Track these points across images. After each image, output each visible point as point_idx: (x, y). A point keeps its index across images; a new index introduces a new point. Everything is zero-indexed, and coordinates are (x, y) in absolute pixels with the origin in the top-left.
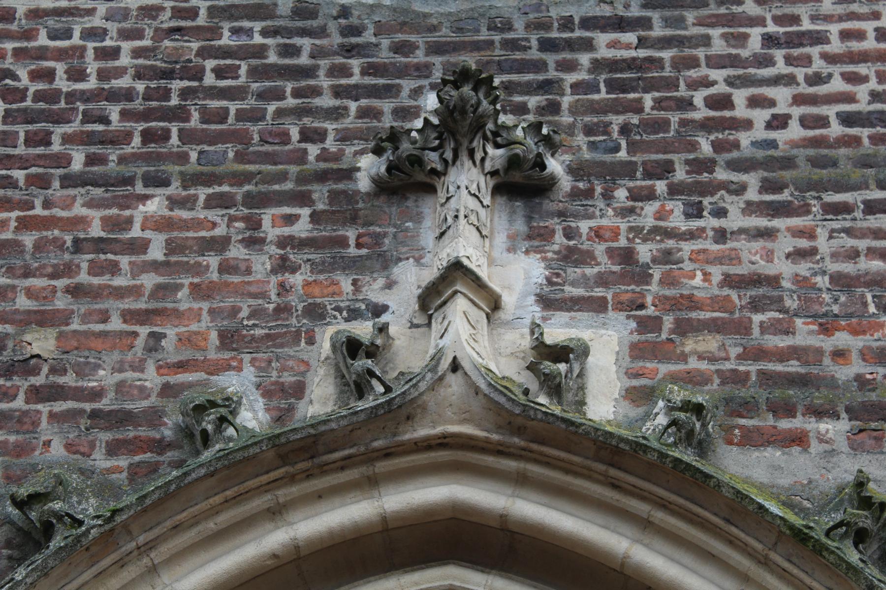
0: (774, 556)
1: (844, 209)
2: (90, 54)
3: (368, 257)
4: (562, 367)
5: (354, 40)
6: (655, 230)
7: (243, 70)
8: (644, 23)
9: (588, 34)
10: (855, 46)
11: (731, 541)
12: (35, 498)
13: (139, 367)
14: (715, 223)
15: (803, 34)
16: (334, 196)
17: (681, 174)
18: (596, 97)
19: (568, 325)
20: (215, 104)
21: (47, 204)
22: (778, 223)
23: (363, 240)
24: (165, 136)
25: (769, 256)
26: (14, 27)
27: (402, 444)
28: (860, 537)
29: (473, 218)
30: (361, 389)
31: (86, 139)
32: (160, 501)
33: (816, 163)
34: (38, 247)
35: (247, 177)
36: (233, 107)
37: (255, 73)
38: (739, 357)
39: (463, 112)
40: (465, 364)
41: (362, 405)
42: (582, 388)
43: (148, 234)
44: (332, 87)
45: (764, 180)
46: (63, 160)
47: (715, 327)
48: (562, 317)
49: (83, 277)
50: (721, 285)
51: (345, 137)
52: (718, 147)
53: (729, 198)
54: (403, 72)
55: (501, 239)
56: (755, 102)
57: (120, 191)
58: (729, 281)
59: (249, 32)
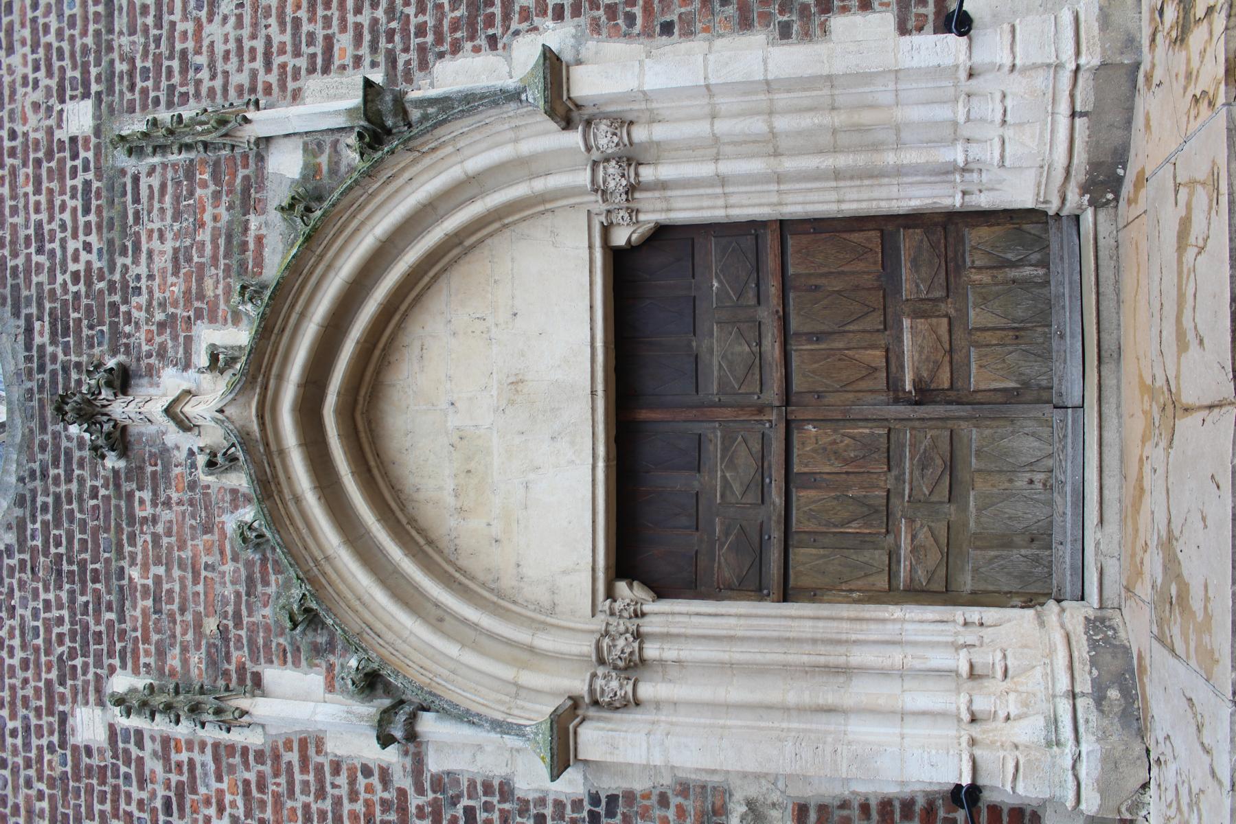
0: (317, 253)
1: (137, 215)
2: (48, 615)
3: (162, 460)
4: (221, 357)
5: (38, 473)
6: (147, 311)
7: (56, 532)
8: (29, 318)
9: (35, 348)
10: (44, 206)
11: (311, 273)
12: (292, 619)
13: (223, 574)
14: (144, 280)
15: (36, 233)
16: (128, 479)
17: (117, 298)
18: (72, 343)
19: (199, 355)
20: (76, 546)
21: (135, 630)
22: (144, 247)
23: (153, 462)
24: (95, 571)
25: (162, 253)
26: (32, 658)
27: (262, 437)
28: (308, 210)
29: (140, 405)
30: (234, 459)
31: (97, 612)
32: (292, 556)
33: (111, 228)
34: (158, 631)
35: (118, 526)
36: (78, 536)
37: (58, 525)
38: (216, 268)
39: (80, 409)
40: (220, 406)
41: (242, 458)
42: (232, 348)
43: (151, 575)
44: (66, 483)
45: (120, 255)
46: (110, 624)
47: (200, 280)
48: (195, 359)
49: (175, 607)
50: (178, 277)
51: (95, 475)
52: (101, 279)
53: (130, 273)
54: (57, 446)
55: (152, 391)
56: (76, 259)
57: (127, 592)
58: (176, 273)
59: (34, 531)
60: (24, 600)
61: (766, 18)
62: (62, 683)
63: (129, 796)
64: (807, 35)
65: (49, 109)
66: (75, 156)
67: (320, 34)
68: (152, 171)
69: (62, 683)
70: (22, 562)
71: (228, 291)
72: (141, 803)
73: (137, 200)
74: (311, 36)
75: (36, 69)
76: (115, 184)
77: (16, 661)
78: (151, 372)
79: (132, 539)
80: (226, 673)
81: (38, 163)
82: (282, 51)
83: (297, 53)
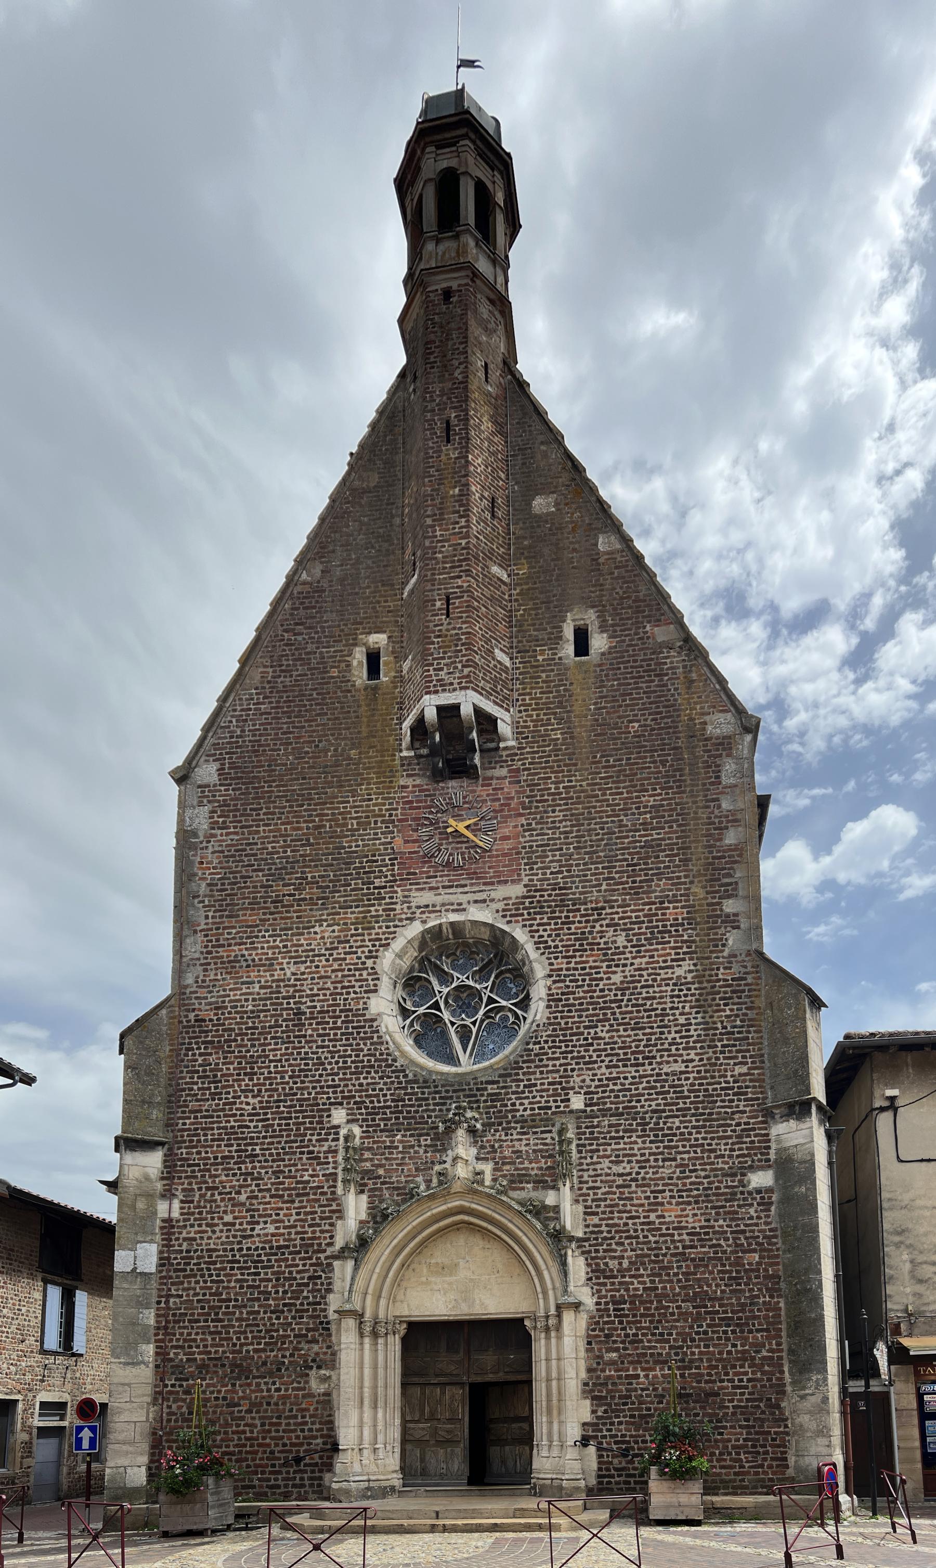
1: (536, 1133)
8: (498, 1082)
37: (416, 1100)
46: (379, 1125)
51: (436, 1117)
54: (447, 1098)
56: (522, 1104)
60: (385, 1084)
61: (591, 1378)
62: (355, 1103)
63: (312, 1135)
64: (584, 1392)
65: (581, 1087)
66: (562, 1101)
67: (599, 1210)
68: (553, 1139)
69: (355, 1103)
70: (400, 1083)
71: (504, 1176)
72: (310, 1140)
73: (542, 1132)
74: (599, 1206)
75: (600, 1080)
76: (548, 1121)
77: (362, 1081)
78: (476, 1142)
79: (411, 1135)
80: (363, 1178)
81: (561, 1083)
82: (595, 1194)
83: (593, 1201)
